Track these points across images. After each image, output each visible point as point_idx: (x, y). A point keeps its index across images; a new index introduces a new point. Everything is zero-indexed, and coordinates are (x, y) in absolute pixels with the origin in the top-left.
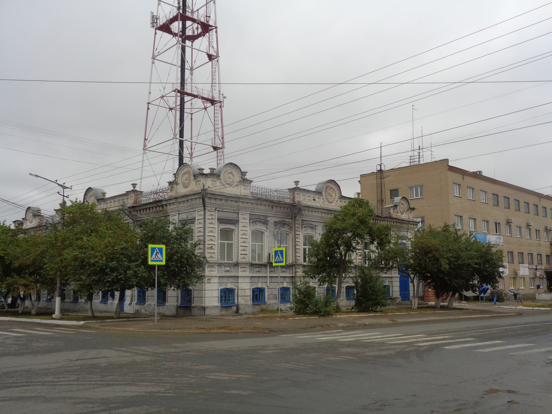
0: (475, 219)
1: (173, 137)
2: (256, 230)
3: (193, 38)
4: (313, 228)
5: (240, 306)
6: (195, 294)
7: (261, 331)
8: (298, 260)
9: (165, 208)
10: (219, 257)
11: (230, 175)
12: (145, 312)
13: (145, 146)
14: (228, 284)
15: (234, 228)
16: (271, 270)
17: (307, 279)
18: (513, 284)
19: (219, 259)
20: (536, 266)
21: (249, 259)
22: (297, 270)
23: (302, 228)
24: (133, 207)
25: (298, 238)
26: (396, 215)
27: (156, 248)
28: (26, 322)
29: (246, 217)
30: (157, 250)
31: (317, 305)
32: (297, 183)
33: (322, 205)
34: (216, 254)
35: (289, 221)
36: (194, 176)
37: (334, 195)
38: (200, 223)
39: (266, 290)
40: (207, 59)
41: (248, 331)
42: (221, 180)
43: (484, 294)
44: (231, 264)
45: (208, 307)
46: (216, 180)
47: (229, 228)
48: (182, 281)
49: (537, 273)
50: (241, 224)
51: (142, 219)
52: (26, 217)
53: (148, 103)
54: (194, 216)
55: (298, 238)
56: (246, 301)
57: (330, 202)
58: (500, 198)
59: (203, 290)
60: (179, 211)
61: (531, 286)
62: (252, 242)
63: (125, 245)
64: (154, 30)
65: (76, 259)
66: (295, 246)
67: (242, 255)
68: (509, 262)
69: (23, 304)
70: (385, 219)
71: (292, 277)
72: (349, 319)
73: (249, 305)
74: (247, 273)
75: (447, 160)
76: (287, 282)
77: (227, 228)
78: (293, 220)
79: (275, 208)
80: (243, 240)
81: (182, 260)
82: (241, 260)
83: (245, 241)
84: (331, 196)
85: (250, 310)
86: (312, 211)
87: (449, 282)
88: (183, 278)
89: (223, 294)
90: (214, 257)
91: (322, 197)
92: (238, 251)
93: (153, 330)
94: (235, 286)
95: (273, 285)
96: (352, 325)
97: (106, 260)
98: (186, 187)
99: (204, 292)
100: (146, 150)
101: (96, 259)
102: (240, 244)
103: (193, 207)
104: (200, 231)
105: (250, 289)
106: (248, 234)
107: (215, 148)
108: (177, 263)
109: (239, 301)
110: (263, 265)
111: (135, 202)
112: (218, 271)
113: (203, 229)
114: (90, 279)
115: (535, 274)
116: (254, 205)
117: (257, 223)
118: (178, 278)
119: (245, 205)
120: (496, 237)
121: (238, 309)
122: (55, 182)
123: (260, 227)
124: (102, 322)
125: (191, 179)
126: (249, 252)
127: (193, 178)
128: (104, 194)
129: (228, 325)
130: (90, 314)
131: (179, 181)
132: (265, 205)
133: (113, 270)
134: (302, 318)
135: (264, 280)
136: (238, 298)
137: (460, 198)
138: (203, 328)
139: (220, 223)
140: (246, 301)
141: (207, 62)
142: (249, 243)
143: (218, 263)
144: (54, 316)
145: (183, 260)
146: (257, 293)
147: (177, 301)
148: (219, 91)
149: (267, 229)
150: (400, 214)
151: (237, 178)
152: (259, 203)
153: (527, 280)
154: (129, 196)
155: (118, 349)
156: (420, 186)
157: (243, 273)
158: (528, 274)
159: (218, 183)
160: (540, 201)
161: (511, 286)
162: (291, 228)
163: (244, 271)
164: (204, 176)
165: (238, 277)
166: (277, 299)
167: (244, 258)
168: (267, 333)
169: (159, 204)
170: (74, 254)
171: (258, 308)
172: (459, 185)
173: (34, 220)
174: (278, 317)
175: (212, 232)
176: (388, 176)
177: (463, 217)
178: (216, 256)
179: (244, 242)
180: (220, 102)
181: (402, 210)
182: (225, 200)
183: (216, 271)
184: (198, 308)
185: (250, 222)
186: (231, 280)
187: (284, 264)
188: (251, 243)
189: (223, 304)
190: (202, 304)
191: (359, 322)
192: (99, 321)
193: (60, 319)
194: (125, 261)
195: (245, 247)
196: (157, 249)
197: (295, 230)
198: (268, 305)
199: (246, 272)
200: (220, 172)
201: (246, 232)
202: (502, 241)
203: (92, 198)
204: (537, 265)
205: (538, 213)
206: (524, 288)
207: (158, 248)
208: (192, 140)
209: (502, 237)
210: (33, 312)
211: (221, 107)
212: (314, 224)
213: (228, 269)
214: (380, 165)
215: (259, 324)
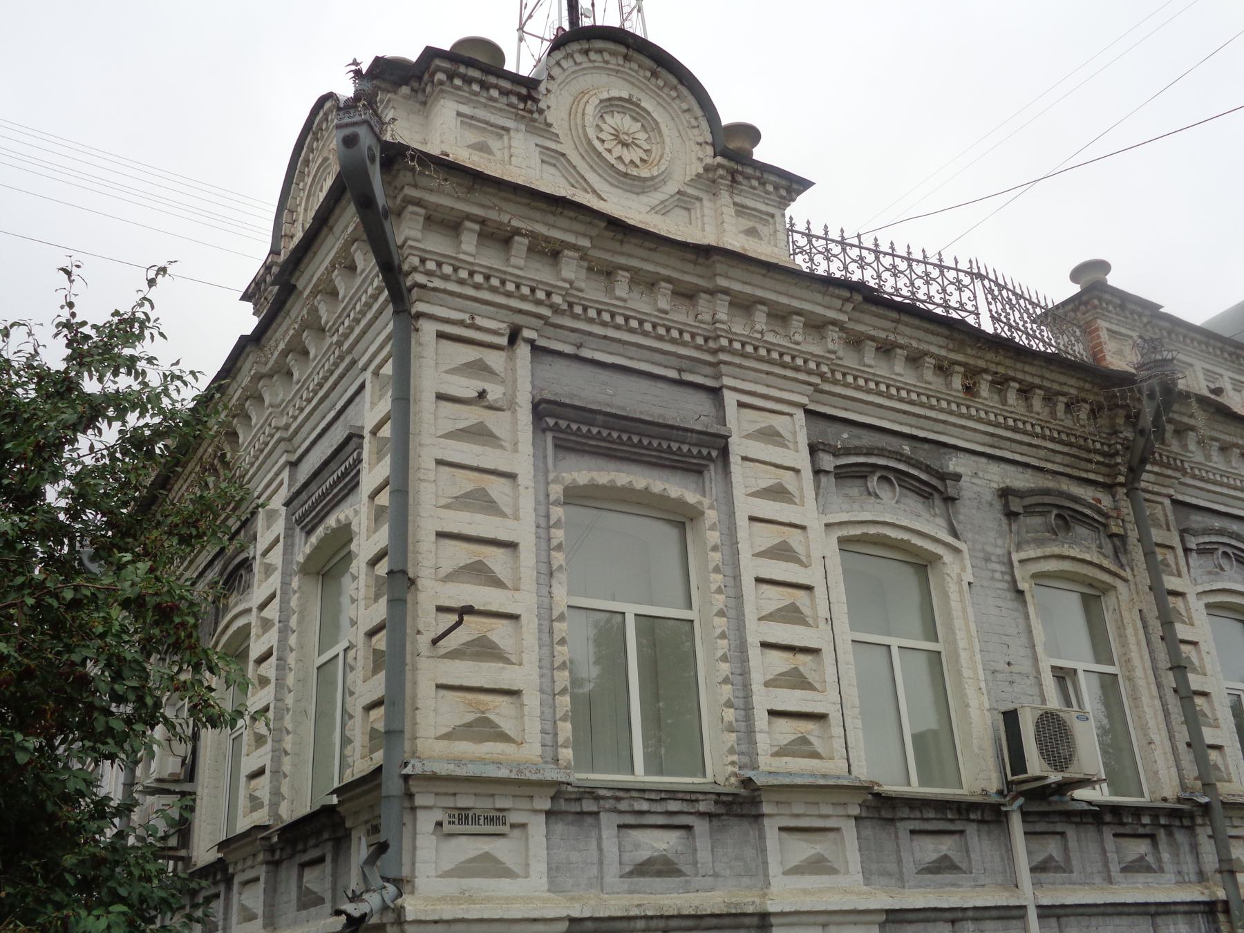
2: (872, 530)
10: (566, 729)
11: (624, 122)
15: (691, 498)
16: (1040, 857)
29: (779, 423)
34: (532, 700)
42: (555, 137)
44: (690, 797)
46: (509, 123)
67: (783, 724)
74: (841, 880)
78: (1121, 491)
90: (507, 726)
92: (746, 687)
106: (816, 555)
110: (973, 806)
112: (554, 870)
117: (873, 482)
132: (915, 360)
139: (557, 446)
142: (830, 620)
143: (558, 791)
149: (955, 534)
162: (1118, 542)
163: (817, 866)
164: (405, 90)
167: (801, 747)
178: (533, 728)
183: (539, 868)
185: (817, 472)
195: (807, 659)
197: (1149, 555)
199: (833, 871)
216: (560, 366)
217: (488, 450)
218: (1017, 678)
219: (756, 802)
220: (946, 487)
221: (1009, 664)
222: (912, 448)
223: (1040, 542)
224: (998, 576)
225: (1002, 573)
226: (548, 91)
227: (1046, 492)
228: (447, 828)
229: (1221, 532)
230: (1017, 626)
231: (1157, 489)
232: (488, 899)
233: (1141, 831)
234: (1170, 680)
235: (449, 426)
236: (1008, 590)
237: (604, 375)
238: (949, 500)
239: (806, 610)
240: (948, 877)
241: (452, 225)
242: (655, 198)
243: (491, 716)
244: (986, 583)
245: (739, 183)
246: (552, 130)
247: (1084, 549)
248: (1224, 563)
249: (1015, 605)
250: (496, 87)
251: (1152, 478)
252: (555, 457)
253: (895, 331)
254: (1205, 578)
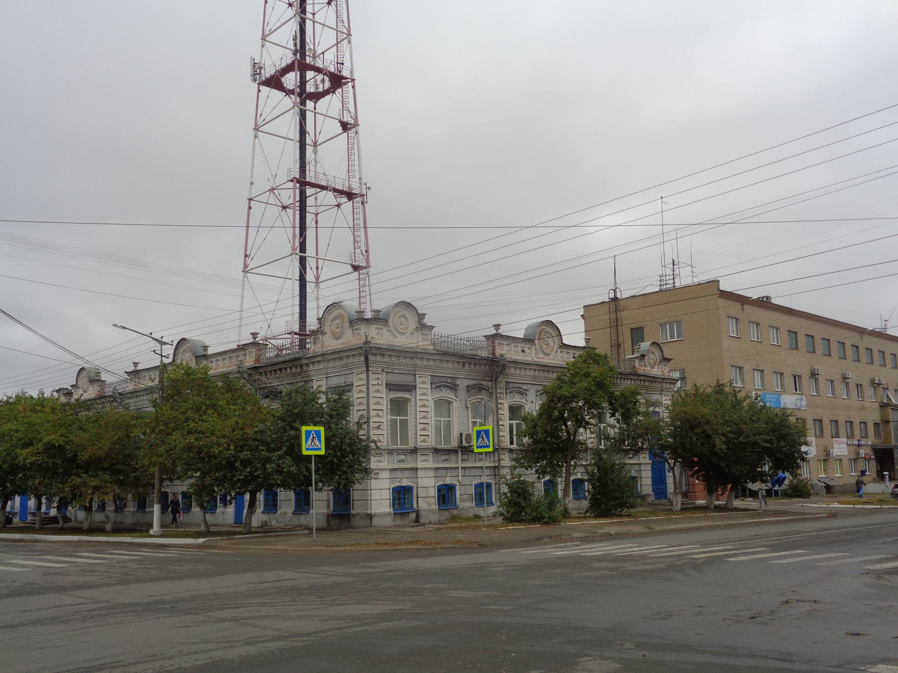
0: (762, 371)
1: (291, 252)
2: (440, 398)
3: (316, 96)
4: (523, 393)
5: (421, 512)
6: (356, 495)
7: (468, 546)
8: (502, 441)
9: (306, 369)
10: (390, 440)
11: (402, 319)
12: (277, 524)
13: (246, 266)
14: (404, 479)
15: (410, 397)
17: (518, 471)
18: (824, 470)
19: (390, 444)
20: (859, 440)
21: (432, 442)
22: (502, 457)
23: (506, 393)
24: (255, 368)
25: (501, 409)
26: (644, 370)
27: (311, 431)
28: (107, 542)
29: (425, 380)
30: (313, 434)
31: (538, 507)
32: (497, 326)
33: (535, 360)
34: (385, 436)
35: (488, 384)
36: (351, 322)
37: (551, 343)
38: (360, 391)
39: (458, 488)
40: (340, 129)
41: (449, 546)
43: (780, 487)
44: (407, 450)
45: (376, 515)
47: (403, 398)
48: (344, 477)
49: (861, 451)
50: (419, 391)
51: (269, 385)
52: (76, 384)
53: (250, 200)
54: (350, 380)
55: (501, 409)
56: (429, 504)
57: (546, 354)
58: (799, 338)
59: (368, 490)
60: (327, 374)
61: (852, 473)
62: (435, 417)
63: (261, 426)
64: (256, 85)
65: (189, 448)
66: (498, 421)
68: (816, 436)
69: (90, 516)
70: (630, 377)
71: (494, 467)
72: (585, 527)
73: (434, 511)
74: (429, 463)
75: (716, 282)
77: (400, 398)
79: (467, 366)
80: (422, 414)
81: (342, 446)
82: (420, 445)
83: (425, 416)
84: (547, 344)
85: (435, 518)
86: (520, 368)
87: (727, 470)
88: (345, 472)
89: (396, 495)
90: (382, 440)
91: (534, 347)
92: (416, 431)
93: (315, 548)
94: (413, 483)
95: (466, 481)
96: (593, 535)
97: (235, 449)
98: (337, 338)
99: (369, 493)
100: (247, 272)
101: (221, 448)
102: (419, 421)
103: (350, 367)
104: (360, 404)
105: (435, 487)
106: (430, 405)
107: (356, 268)
108: (335, 451)
109: (420, 505)
110: (452, 450)
111: (258, 359)
112: (388, 461)
113: (365, 399)
114: (211, 477)
115: (858, 453)
116: (437, 362)
117: (442, 388)
118: (339, 473)
119: (425, 362)
120: (796, 397)
121: (418, 517)
122: (149, 335)
123: (446, 394)
124: (230, 539)
125: (345, 325)
126: (431, 431)
127: (348, 324)
128: (206, 348)
129: (418, 539)
130: (203, 528)
131: (327, 329)
132: (453, 362)
133: (245, 463)
134: (518, 527)
135: (454, 472)
136: (417, 500)
137: (737, 339)
138: (386, 544)
140: (429, 504)
141: (339, 133)
142: (431, 418)
144: (151, 532)
145: (344, 447)
146: (444, 493)
147: (328, 507)
148: (360, 179)
149: (456, 397)
150: (649, 368)
151: (413, 323)
152: (444, 359)
153: (846, 462)
154: (248, 351)
155: (296, 570)
156: (676, 322)
157: (424, 463)
158: (846, 453)
160: (862, 339)
161: (821, 472)
162: (491, 394)
163: (425, 460)
164: (365, 322)
165: (416, 469)
166: (473, 500)
167: (424, 441)
168: (476, 548)
169: (296, 363)
170: (186, 441)
171: (446, 515)
172: (737, 319)
173: (91, 388)
174: (484, 526)
175: (378, 403)
176: (626, 308)
177: (744, 369)
178: (385, 440)
179: (425, 417)
180: (362, 195)
181: (652, 362)
182: (396, 356)
183: (386, 461)
184: (361, 516)
185: (432, 388)
186: (406, 474)
187: (491, 449)
188: (434, 419)
189: (396, 510)
190: (367, 510)
191: (601, 531)
192: (225, 538)
193: (163, 536)
194: (262, 450)
195: (426, 425)
196: (313, 432)
197: (497, 397)
198: (461, 509)
199: (427, 461)
200: (388, 315)
201: (426, 403)
202: (804, 403)
203: (187, 354)
204: (860, 439)
205: (858, 357)
206: (841, 476)
207: (315, 431)
208: (317, 255)
209: (804, 397)
210: (108, 527)
211: (363, 203)
212: (524, 387)
213: (402, 457)
214: (615, 291)
215: (460, 536)
219: (417, 450)
223: (473, 396)
227: (477, 384)
229: (516, 388)
232: (380, 466)
234: (496, 423)
237: (396, 375)
239: (427, 416)
240: (447, 462)
248: (516, 395)
249: (466, 410)
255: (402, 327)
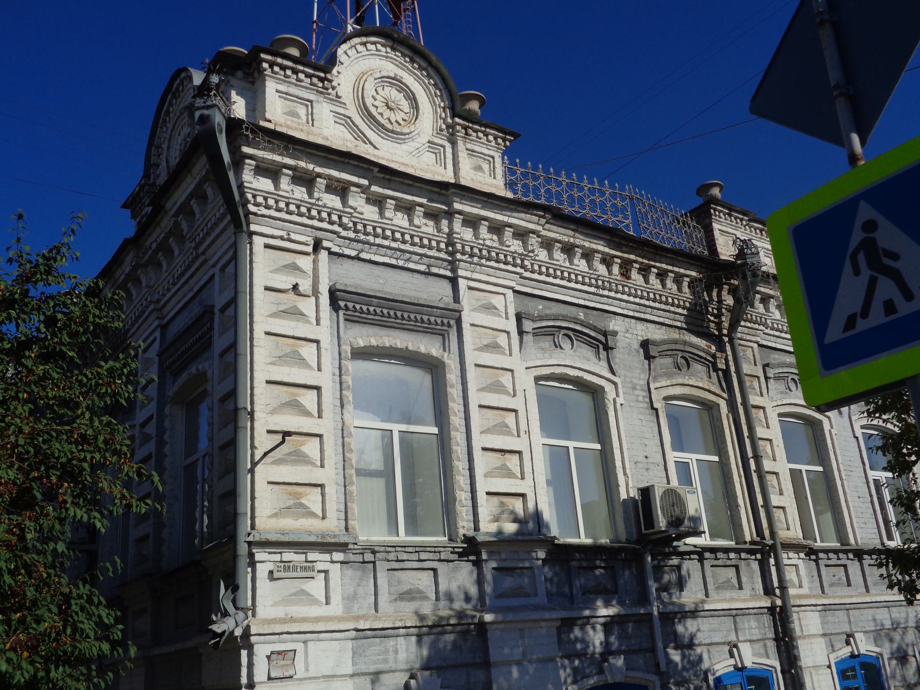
2: (558, 370)
29: (498, 301)
76: (751, 641)
149: (613, 373)
159: (324, 110)
164: (240, 74)
185: (521, 333)
201: (506, 379)
216: (348, 263)
217: (300, 324)
218: (651, 467)
220: (607, 340)
221: (646, 457)
222: (585, 315)
223: (669, 376)
224: (641, 399)
225: (643, 396)
226: (339, 73)
227: (675, 342)
228: (276, 575)
230: (652, 432)
231: (748, 337)
232: (304, 620)
233: (729, 563)
235: (274, 309)
236: (648, 408)
238: (607, 348)
241: (272, 172)
242: (410, 146)
243: (304, 501)
244: (632, 404)
245: (470, 135)
246: (341, 100)
247: (699, 379)
248: (792, 386)
250: (303, 72)
251: (746, 330)
252: (345, 326)
253: (574, 237)
254: (779, 396)
255: (399, 116)
